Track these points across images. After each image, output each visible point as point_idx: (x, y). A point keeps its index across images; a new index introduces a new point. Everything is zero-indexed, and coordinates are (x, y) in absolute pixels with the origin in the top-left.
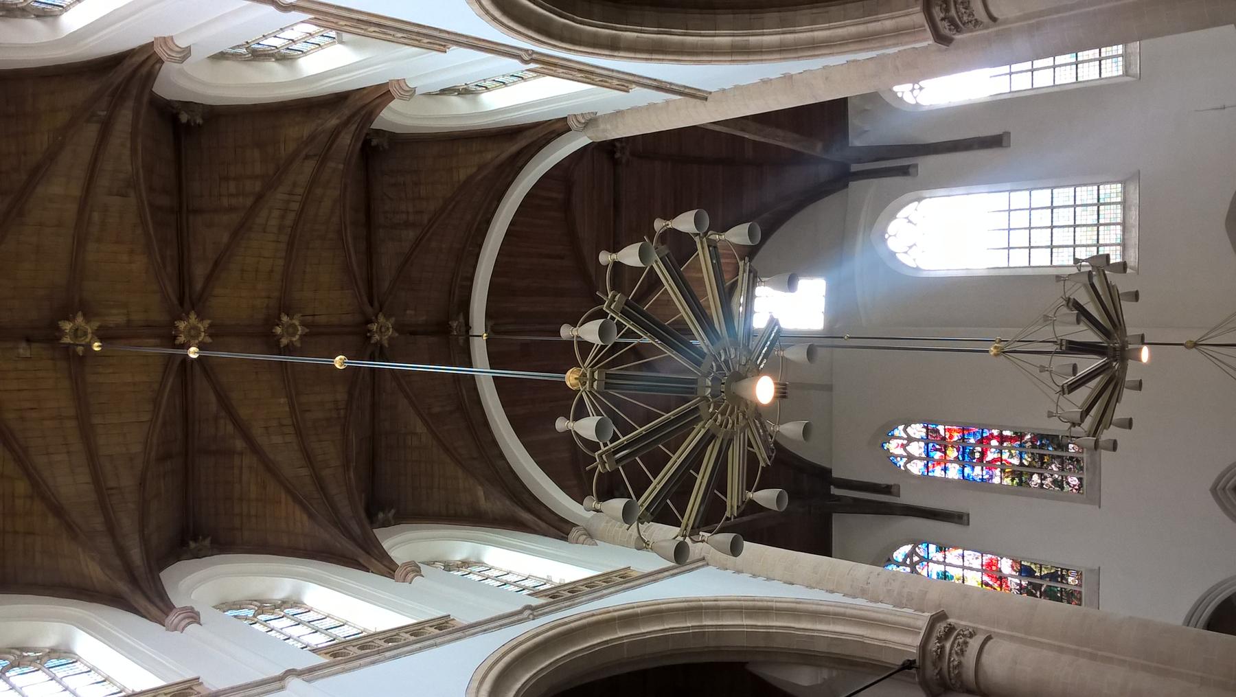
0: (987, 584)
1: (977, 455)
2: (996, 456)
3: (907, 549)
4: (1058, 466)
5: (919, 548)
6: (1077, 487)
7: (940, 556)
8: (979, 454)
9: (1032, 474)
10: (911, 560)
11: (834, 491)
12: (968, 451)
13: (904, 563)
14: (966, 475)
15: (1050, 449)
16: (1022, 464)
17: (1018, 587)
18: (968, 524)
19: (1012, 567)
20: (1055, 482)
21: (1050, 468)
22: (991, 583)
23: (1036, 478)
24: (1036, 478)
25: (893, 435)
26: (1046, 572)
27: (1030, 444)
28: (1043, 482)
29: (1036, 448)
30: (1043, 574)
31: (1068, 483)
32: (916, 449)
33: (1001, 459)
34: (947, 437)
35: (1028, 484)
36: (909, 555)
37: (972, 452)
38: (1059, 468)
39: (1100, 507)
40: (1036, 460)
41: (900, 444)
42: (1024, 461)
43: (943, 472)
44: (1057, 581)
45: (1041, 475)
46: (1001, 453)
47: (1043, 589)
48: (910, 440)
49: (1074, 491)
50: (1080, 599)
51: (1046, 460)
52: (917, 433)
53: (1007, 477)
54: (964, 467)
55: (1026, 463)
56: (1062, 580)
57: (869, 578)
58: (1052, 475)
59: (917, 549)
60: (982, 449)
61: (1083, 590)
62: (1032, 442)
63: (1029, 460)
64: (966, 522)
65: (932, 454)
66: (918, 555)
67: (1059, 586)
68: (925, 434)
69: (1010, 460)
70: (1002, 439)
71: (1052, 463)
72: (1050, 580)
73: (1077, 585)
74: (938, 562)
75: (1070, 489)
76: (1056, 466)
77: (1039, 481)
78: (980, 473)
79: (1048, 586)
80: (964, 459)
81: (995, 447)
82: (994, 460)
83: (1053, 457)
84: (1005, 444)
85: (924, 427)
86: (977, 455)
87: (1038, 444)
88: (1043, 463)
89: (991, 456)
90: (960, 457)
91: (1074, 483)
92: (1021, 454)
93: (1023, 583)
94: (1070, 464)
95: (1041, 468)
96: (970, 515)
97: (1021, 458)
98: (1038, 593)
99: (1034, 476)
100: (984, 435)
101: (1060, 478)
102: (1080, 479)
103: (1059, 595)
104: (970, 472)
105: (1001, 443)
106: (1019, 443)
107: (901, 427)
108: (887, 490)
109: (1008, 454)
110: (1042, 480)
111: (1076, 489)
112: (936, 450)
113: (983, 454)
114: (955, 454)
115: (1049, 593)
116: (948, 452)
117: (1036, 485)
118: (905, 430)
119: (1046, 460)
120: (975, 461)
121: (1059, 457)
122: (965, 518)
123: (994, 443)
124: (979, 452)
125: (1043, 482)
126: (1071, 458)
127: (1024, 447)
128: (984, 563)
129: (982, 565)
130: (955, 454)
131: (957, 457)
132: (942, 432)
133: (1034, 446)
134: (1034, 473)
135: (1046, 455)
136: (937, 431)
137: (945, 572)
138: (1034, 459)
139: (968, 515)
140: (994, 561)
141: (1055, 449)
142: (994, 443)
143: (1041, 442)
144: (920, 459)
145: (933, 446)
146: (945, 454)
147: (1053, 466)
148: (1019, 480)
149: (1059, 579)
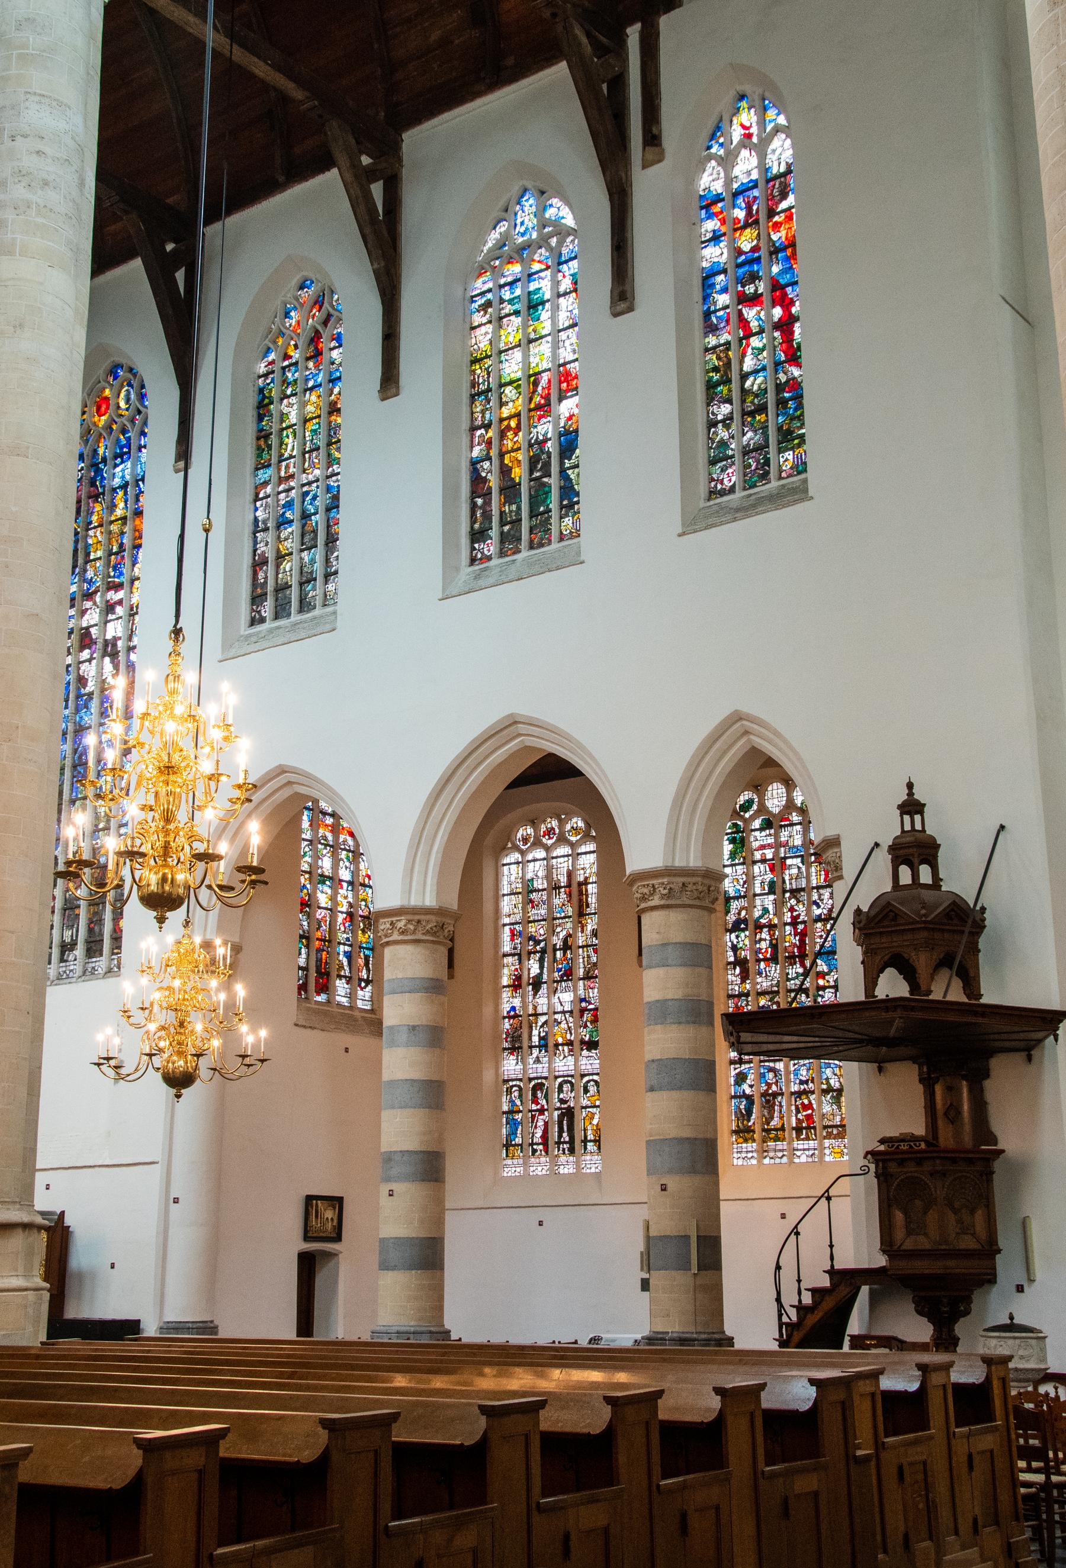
0: (536, 384)
1: (750, 289)
2: (754, 325)
3: (569, 221)
4: (752, 442)
5: (573, 241)
6: (719, 487)
7: (566, 284)
8: (752, 291)
9: (729, 401)
10: (551, 236)
11: (633, 33)
12: (756, 267)
13: (543, 224)
14: (712, 280)
15: (781, 419)
16: (744, 377)
17: (541, 438)
18: (615, 315)
19: (570, 418)
20: (724, 444)
21: (746, 429)
22: (540, 389)
23: (726, 409)
24: (726, 409)
25: (765, 109)
26: (572, 477)
27: (783, 378)
28: (720, 425)
29: (777, 394)
30: (570, 472)
31: (723, 470)
32: (746, 166)
33: (749, 334)
34: (776, 219)
35: (713, 399)
36: (563, 232)
37: (754, 277)
38: (748, 445)
39: (679, 535)
40: (756, 401)
41: (751, 131)
42: (751, 379)
43: (709, 236)
44: (561, 500)
45: (730, 417)
46: (761, 331)
47: (545, 480)
48: (761, 150)
49: (713, 484)
50: (541, 545)
51: (758, 418)
52: (775, 157)
53: (719, 358)
54: (724, 271)
55: (748, 384)
56: (566, 506)
57: (25, 136)
58: (733, 437)
59: (571, 238)
60: (761, 295)
61: (555, 546)
62: (788, 381)
63: (755, 388)
64: (619, 309)
65: (740, 201)
66: (560, 243)
67: (554, 506)
68: (775, 171)
69: (749, 351)
70: (786, 325)
71: (755, 431)
72: (561, 488)
73: (561, 533)
74: (556, 283)
75: (715, 476)
76: (751, 439)
77: (720, 417)
78: (719, 305)
79: (550, 486)
80: (739, 266)
81: (769, 315)
82: (744, 323)
83: (765, 428)
84: (777, 334)
85: (789, 165)
86: (750, 289)
87: (787, 395)
88: (752, 414)
89: (750, 314)
90: (743, 257)
91: (726, 481)
92: (764, 369)
93: (549, 444)
94: (758, 462)
95: (744, 413)
96: (630, 314)
97: (756, 372)
98: (538, 474)
99: (727, 405)
100: (789, 289)
101: (730, 453)
102: (732, 490)
103: (542, 509)
104: (718, 287)
105: (777, 326)
106: (783, 358)
107: (782, 120)
108: (652, 139)
109: (761, 345)
110: (723, 421)
111: (716, 486)
112: (749, 208)
113: (754, 300)
114: (746, 247)
115: (541, 493)
116: (748, 230)
117: (713, 413)
118: (777, 130)
119: (758, 418)
120: (740, 288)
121: (767, 440)
122: (623, 306)
123: (778, 312)
124: (756, 290)
125: (720, 425)
126: (767, 462)
127: (776, 371)
128: (568, 366)
129: (564, 365)
130: (746, 247)
131: (740, 252)
132: (784, 205)
133: (779, 388)
134: (731, 404)
135: (767, 416)
136: (784, 196)
137: (543, 303)
138: (757, 396)
139: (631, 309)
140: (574, 383)
141: (780, 429)
142: (778, 312)
143: (791, 399)
144: (729, 180)
145: (755, 198)
146: (746, 225)
147: (750, 434)
148: (718, 380)
149: (565, 502)
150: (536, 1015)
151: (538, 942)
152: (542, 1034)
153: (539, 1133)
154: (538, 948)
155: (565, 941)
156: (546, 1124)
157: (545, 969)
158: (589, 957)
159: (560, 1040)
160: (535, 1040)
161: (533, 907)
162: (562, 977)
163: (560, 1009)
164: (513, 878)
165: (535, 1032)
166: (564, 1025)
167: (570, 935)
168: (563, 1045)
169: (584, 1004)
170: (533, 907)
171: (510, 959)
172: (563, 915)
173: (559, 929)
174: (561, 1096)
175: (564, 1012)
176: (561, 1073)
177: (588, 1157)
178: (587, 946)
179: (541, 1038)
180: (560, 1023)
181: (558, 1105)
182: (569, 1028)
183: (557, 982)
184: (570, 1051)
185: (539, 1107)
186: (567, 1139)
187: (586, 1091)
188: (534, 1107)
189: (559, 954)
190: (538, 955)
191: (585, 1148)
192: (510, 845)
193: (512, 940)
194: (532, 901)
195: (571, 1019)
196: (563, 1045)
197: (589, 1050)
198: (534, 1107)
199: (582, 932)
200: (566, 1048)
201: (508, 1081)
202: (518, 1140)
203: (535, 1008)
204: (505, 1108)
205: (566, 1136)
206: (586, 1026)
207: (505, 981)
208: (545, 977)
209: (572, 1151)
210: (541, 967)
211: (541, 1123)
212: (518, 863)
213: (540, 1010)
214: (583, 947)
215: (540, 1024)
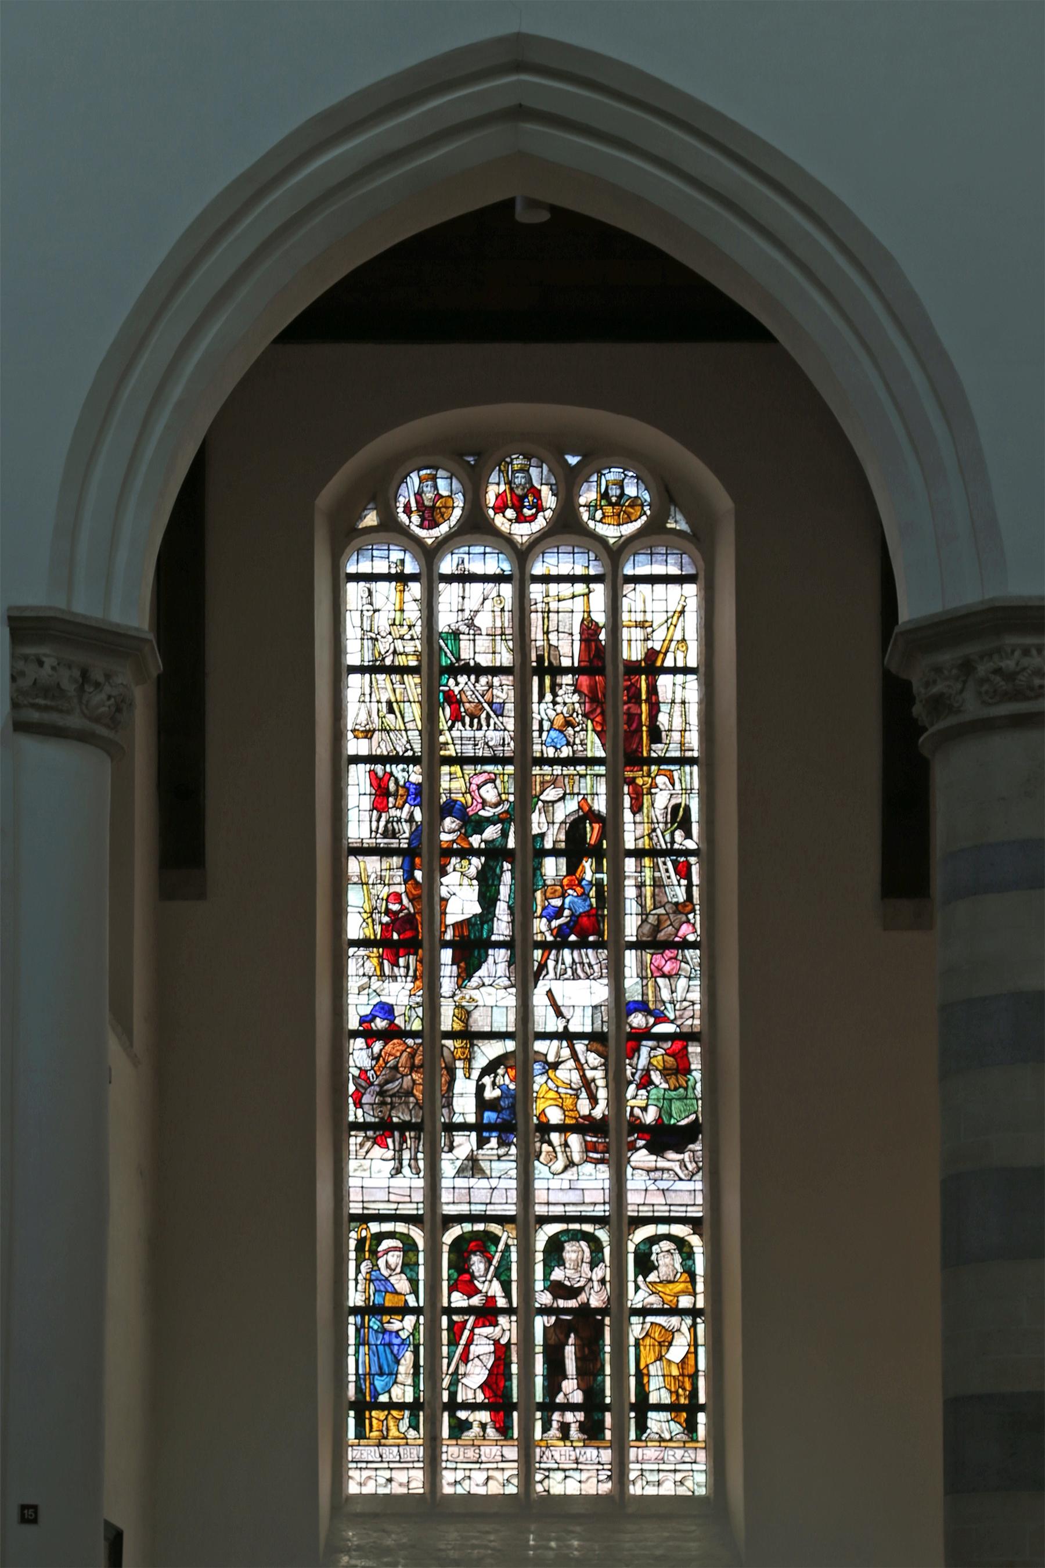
150: (469, 1036)
151: (479, 825)
152: (490, 1094)
153: (476, 1375)
154: (475, 841)
155: (575, 829)
156: (501, 1352)
157: (502, 909)
158: (657, 884)
159: (555, 1116)
160: (465, 1107)
161: (456, 718)
162: (561, 933)
163: (554, 1025)
164: (382, 622)
165: (464, 1088)
166: (567, 1073)
167: (588, 815)
168: (562, 1128)
169: (638, 1020)
170: (456, 718)
171: (373, 864)
172: (566, 752)
173: (550, 794)
174: (557, 1274)
175: (567, 1036)
176: (558, 1210)
177: (651, 1453)
178: (654, 853)
179: (482, 1103)
180: (555, 1066)
181: (544, 1299)
182: (587, 1084)
183: (545, 946)
184: (588, 1148)
185: (476, 1301)
186: (578, 1397)
187: (645, 1265)
188: (459, 1300)
189: (552, 868)
190: (477, 862)
191: (642, 1426)
192: (371, 519)
193: (379, 805)
194: (451, 699)
195: (594, 1059)
196: (562, 1128)
197: (656, 1148)
198: (459, 1300)
199: (636, 809)
200: (574, 1140)
201: (365, 1219)
202: (402, 1393)
203: (464, 1014)
204: (355, 1298)
205: (571, 1390)
206: (646, 1083)
207: (355, 927)
208: (502, 927)
209: (592, 1431)
210: (488, 899)
211: (483, 1348)
212: (402, 579)
213: (480, 1022)
214: (638, 854)
215: (480, 1062)
